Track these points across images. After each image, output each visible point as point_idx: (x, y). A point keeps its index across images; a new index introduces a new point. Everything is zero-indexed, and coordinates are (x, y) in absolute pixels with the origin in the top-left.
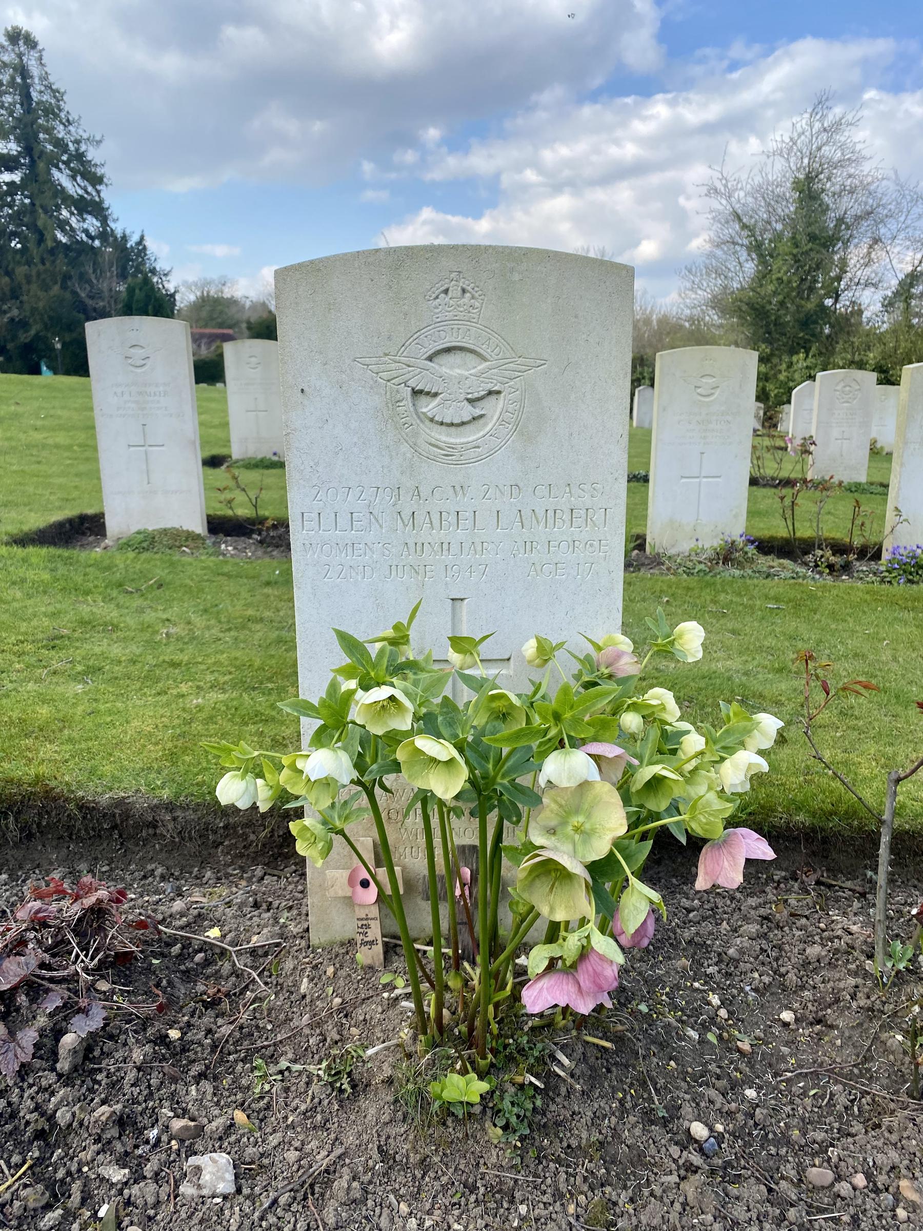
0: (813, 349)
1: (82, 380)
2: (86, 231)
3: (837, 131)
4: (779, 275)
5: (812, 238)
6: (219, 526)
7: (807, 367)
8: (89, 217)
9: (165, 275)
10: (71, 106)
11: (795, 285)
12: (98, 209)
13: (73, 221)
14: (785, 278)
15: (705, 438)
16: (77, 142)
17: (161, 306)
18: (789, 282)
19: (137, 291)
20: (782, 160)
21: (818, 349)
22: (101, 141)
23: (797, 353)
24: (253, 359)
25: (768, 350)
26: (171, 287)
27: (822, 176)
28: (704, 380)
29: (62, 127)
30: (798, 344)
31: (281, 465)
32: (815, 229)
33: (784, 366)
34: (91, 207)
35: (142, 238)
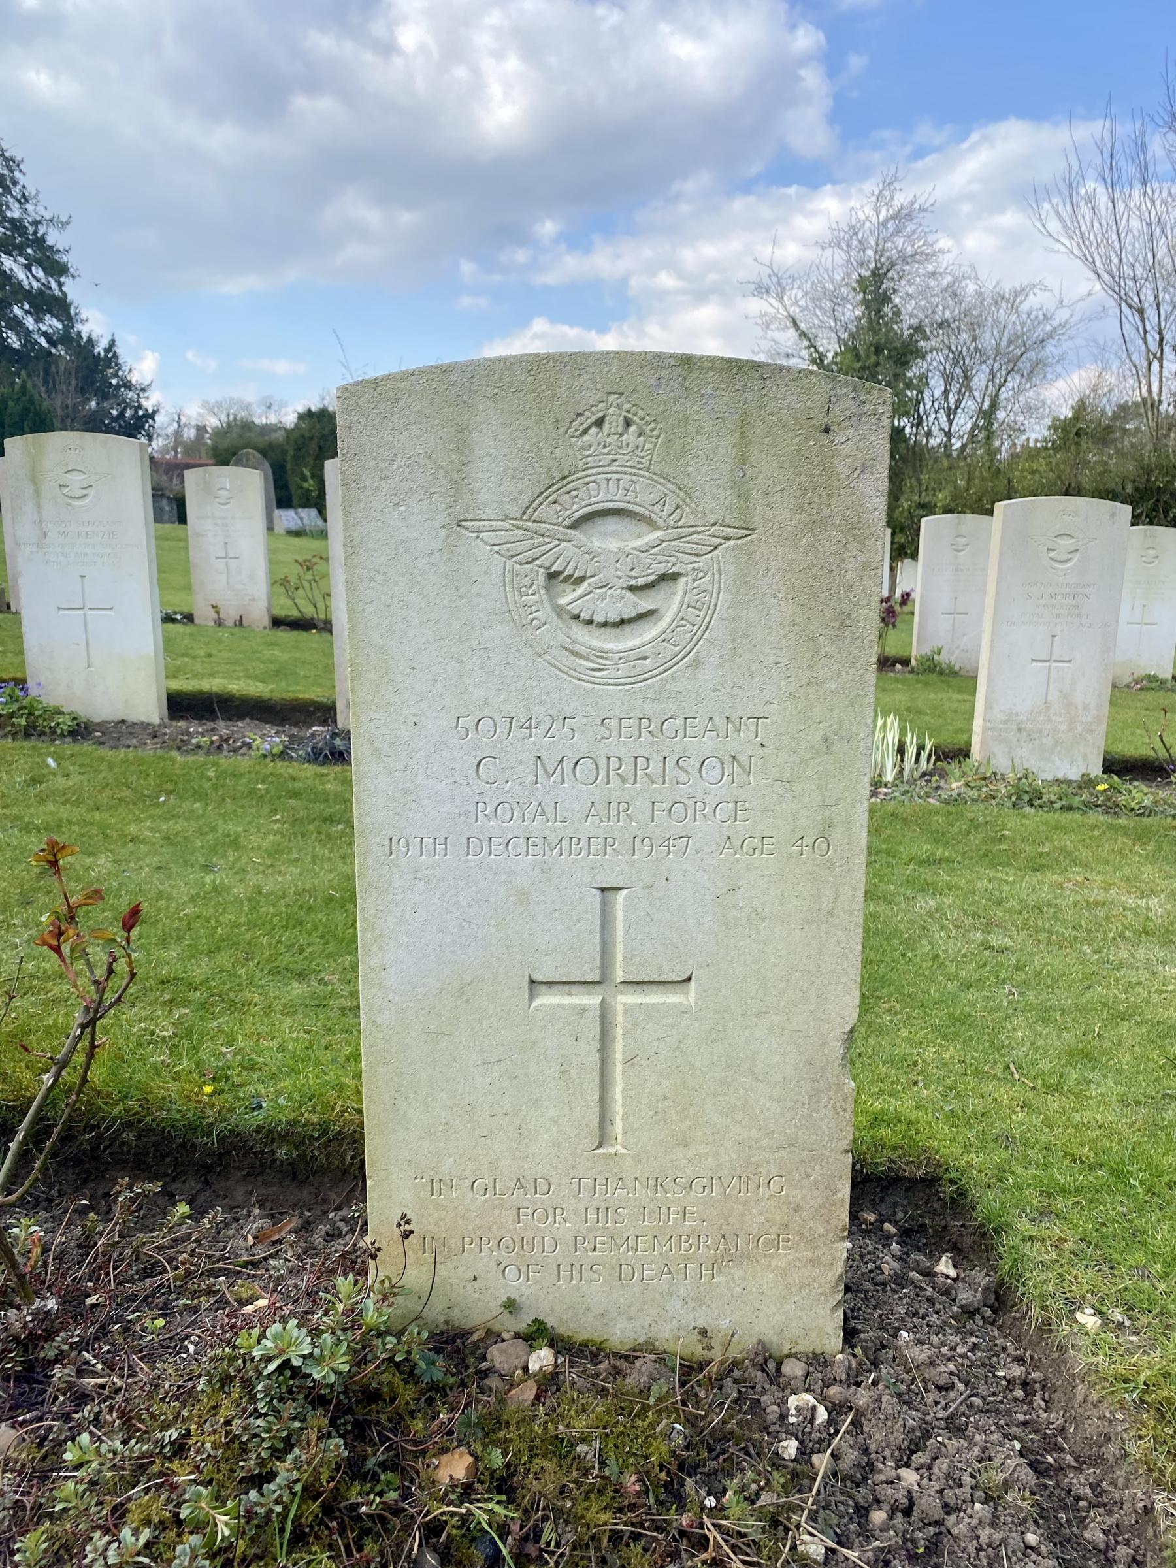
2: (45, 334)
8: (48, 317)
9: (143, 390)
10: (28, 179)
12: (60, 307)
13: (30, 322)
16: (36, 223)
22: (68, 223)
26: (148, 405)
27: (890, 275)
29: (17, 205)
34: (52, 304)
35: (112, 343)
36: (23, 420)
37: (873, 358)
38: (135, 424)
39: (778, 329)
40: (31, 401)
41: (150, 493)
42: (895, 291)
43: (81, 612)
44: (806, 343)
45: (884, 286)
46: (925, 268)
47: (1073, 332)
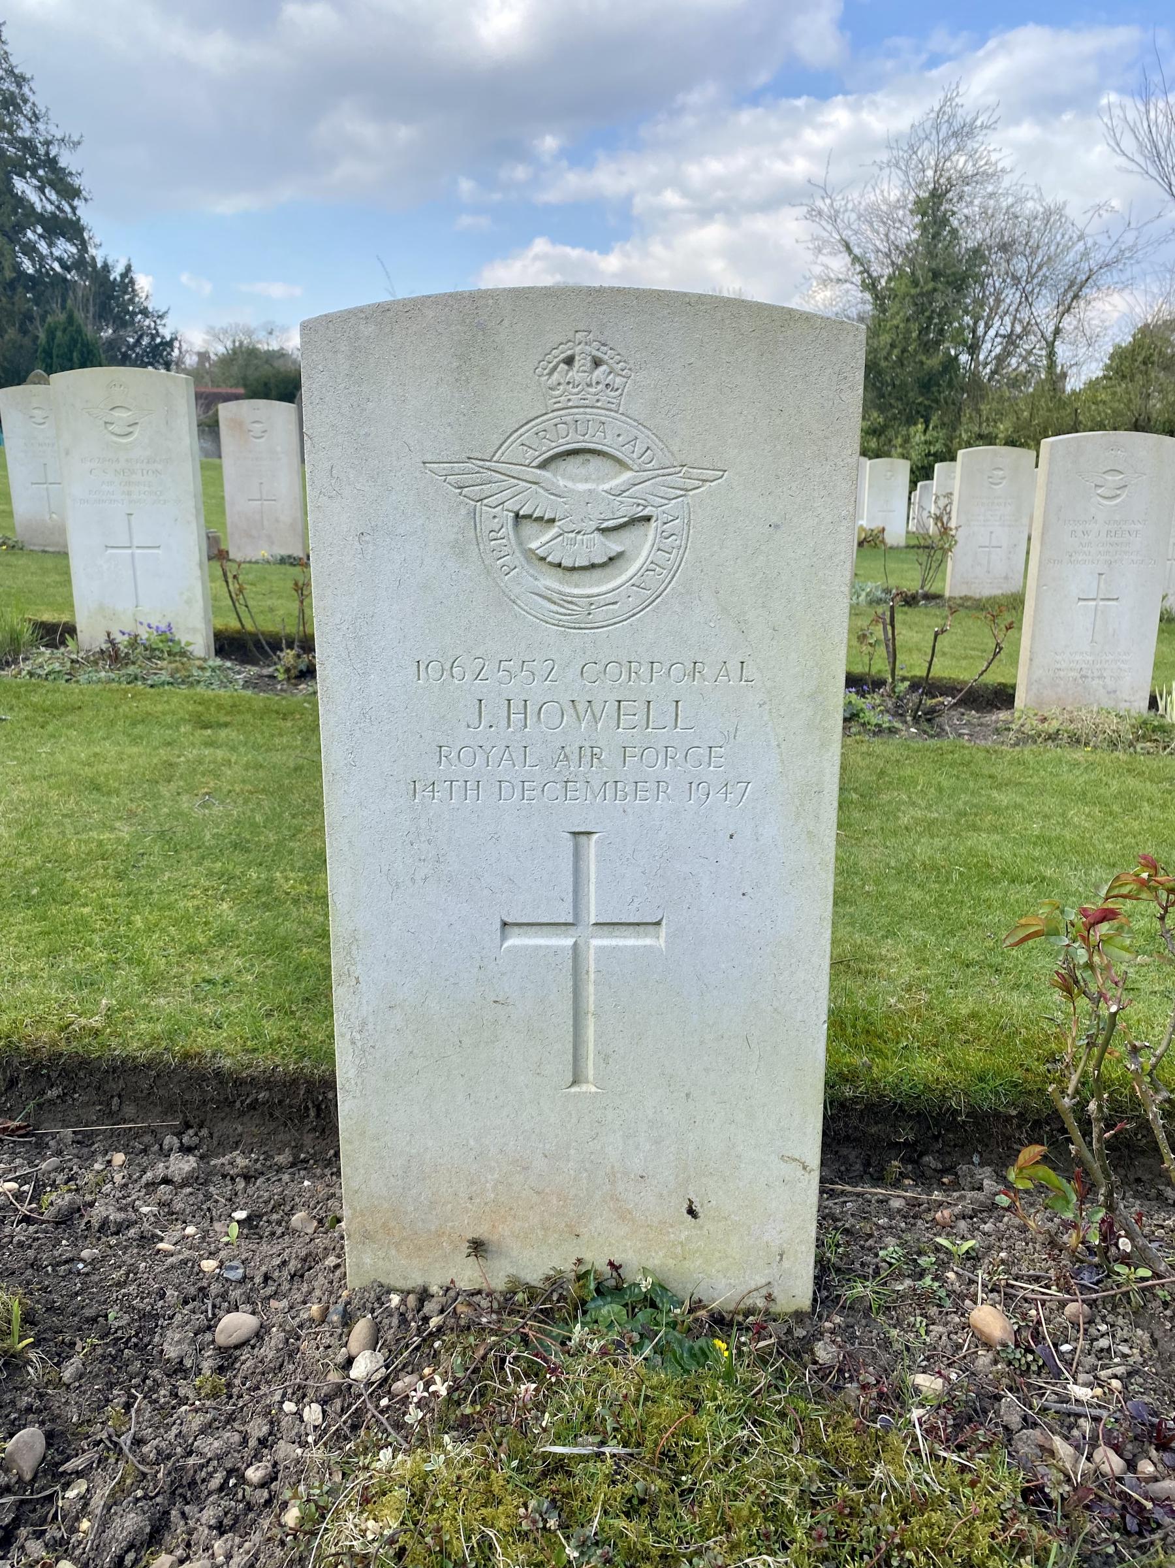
2: (60, 260)
4: (895, 322)
6: (231, 645)
7: (926, 442)
9: (161, 317)
10: (39, 95)
12: (73, 230)
13: (43, 247)
15: (129, 493)
16: (48, 143)
17: (90, 352)
19: (59, 334)
20: (899, 172)
21: (940, 418)
22: (79, 143)
23: (915, 424)
25: (881, 420)
27: (949, 195)
28: (116, 413)
29: (28, 124)
30: (918, 412)
33: (900, 440)
34: (65, 227)
35: (128, 269)
36: (71, 352)
37: (931, 285)
38: (158, 354)
39: (831, 254)
40: (79, 331)
41: (195, 428)
42: (954, 213)
43: (129, 551)
44: (859, 268)
45: (943, 208)
46: (985, 188)
47: (1140, 255)
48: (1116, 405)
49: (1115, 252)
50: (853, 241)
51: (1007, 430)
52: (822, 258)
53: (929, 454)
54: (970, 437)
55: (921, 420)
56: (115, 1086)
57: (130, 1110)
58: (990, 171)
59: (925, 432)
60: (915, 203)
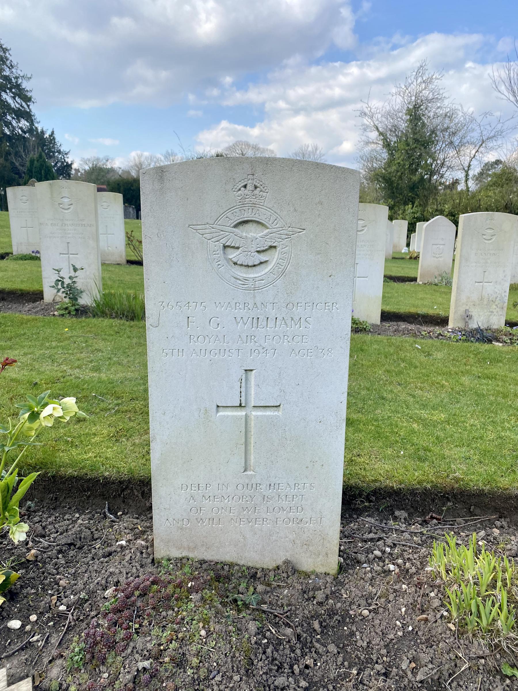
0: (416, 202)
1: (5, 213)
2: (21, 128)
3: (430, 82)
4: (399, 161)
5: (416, 141)
7: (413, 213)
9: (66, 154)
10: (13, 57)
11: (407, 167)
12: (28, 116)
13: (14, 123)
14: (402, 162)
16: (17, 78)
18: (404, 165)
19: (36, 162)
20: (401, 98)
21: (419, 202)
22: (31, 78)
23: (408, 205)
24: (24, 197)
25: (392, 203)
26: (69, 161)
27: (422, 107)
29: (8, 69)
30: (409, 200)
31: (38, 259)
32: (417, 136)
33: (401, 212)
35: (53, 133)
36: (41, 170)
38: (65, 171)
48: (496, 197)
49: (493, 132)
50: (379, 126)
51: (449, 208)
52: (366, 133)
53: (414, 218)
54: (433, 211)
55: (411, 203)
56: (474, 501)
57: (478, 511)
58: (439, 97)
59: (412, 208)
60: (407, 110)
